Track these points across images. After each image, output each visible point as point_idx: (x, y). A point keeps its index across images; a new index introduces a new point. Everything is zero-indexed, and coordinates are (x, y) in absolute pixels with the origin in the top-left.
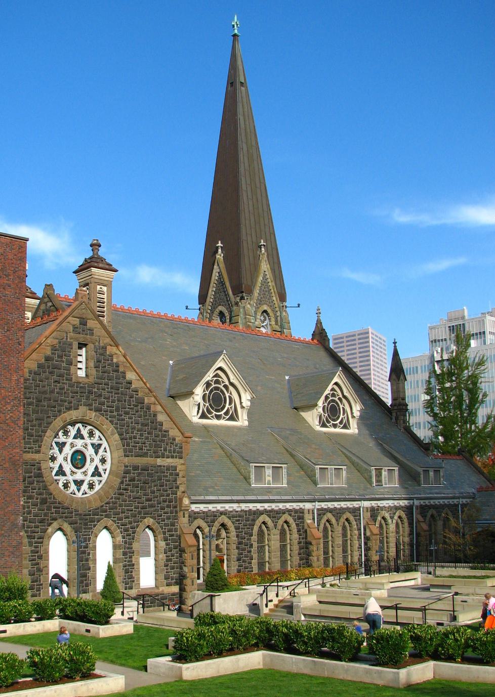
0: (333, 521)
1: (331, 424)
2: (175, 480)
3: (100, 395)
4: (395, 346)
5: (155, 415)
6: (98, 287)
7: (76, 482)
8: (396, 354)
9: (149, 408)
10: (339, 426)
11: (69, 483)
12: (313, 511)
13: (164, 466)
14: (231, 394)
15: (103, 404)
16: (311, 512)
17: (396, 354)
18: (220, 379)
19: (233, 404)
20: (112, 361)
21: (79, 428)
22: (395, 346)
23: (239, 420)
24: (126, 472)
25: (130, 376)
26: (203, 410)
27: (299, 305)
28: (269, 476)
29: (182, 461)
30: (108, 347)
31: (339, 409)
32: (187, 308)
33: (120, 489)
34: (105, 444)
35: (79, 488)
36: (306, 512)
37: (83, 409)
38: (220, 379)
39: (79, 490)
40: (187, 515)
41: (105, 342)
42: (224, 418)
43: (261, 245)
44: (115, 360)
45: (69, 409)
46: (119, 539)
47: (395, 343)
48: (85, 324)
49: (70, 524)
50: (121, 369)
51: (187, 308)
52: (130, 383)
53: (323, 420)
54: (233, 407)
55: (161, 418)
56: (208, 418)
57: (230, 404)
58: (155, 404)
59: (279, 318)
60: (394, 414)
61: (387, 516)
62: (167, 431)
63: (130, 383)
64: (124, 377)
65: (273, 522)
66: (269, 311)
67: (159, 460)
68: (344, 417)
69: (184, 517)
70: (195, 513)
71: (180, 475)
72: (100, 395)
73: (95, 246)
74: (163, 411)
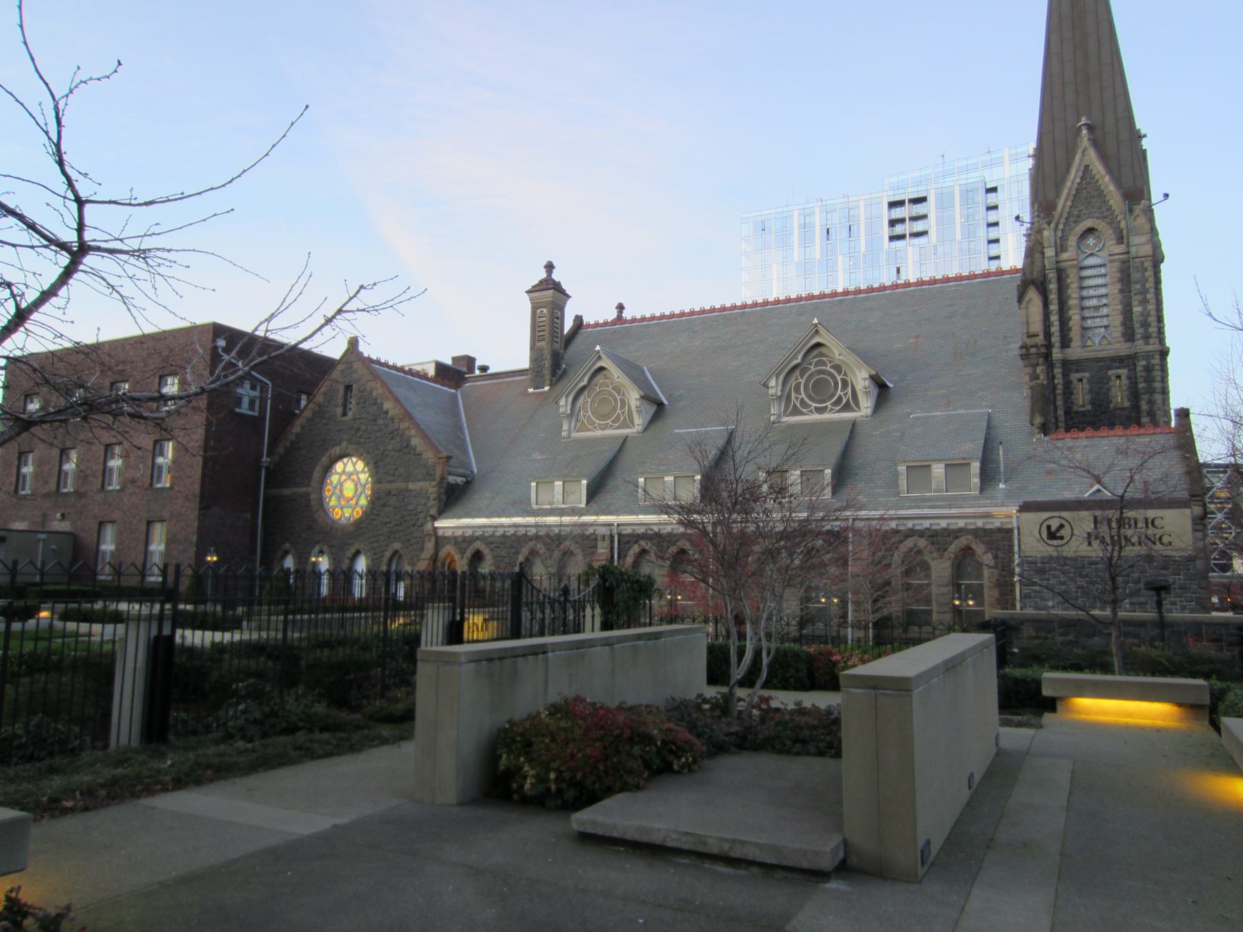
1: (829, 406)
2: (425, 505)
3: (358, 429)
5: (409, 440)
6: (539, 311)
9: (402, 435)
15: (361, 437)
20: (372, 394)
24: (379, 499)
27: (1166, 196)
29: (433, 483)
33: (372, 514)
36: (599, 538)
37: (344, 444)
40: (433, 539)
42: (611, 426)
43: (1080, 127)
44: (374, 394)
45: (333, 446)
46: (369, 561)
48: (351, 368)
49: (329, 547)
50: (379, 401)
52: (387, 412)
53: (795, 405)
55: (415, 441)
57: (623, 406)
58: (409, 428)
59: (1125, 231)
62: (420, 455)
63: (387, 412)
64: (382, 408)
65: (549, 549)
67: (410, 484)
68: (845, 394)
71: (432, 498)
72: (358, 429)
73: (550, 267)
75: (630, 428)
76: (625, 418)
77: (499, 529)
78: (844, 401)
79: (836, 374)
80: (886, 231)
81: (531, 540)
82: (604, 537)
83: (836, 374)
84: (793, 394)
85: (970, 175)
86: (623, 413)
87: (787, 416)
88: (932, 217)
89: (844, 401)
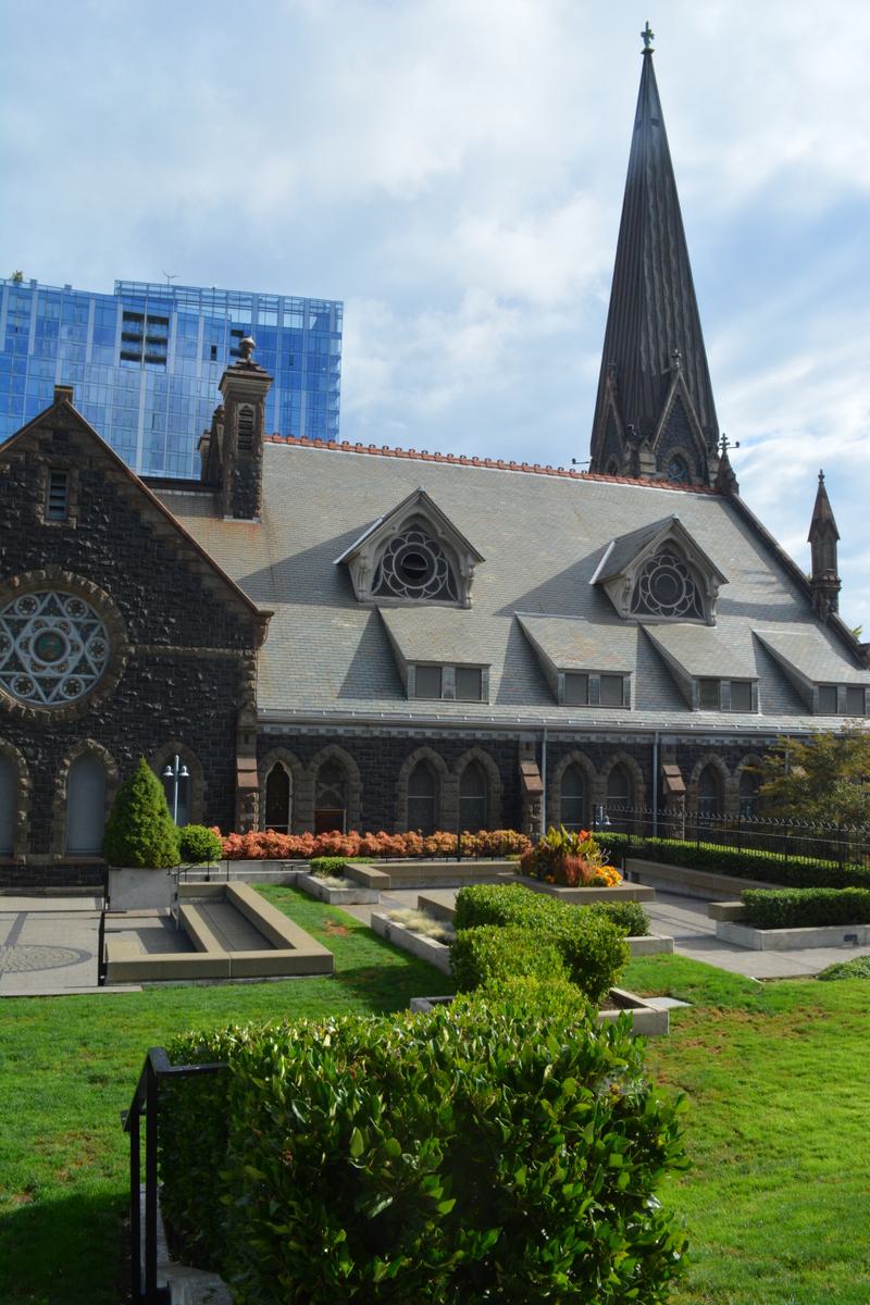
0: (589, 764)
4: (821, 483)
7: (42, 681)
8: (822, 495)
10: (677, 613)
11: (31, 682)
12: (539, 745)
13: (211, 661)
14: (443, 556)
16: (534, 747)
17: (822, 495)
18: (420, 534)
19: (447, 573)
21: (53, 597)
22: (821, 483)
23: (457, 597)
25: (147, 516)
26: (384, 583)
28: (449, 684)
30: (109, 474)
31: (681, 584)
32: (574, 461)
34: (101, 624)
35: (47, 690)
38: (420, 534)
39: (47, 694)
40: (253, 739)
41: (101, 464)
42: (426, 595)
44: (120, 493)
47: (821, 477)
51: (574, 461)
53: (642, 602)
54: (447, 578)
56: (394, 595)
57: (441, 571)
60: (815, 596)
61: (721, 763)
66: (687, 456)
68: (690, 599)
69: (246, 742)
70: (272, 737)
74: (212, 572)
75: (451, 599)
76: (445, 587)
77: (371, 729)
78: (689, 606)
79: (681, 577)
80: (119, 345)
81: (421, 745)
82: (528, 744)
83: (681, 577)
84: (640, 589)
85: (216, 310)
86: (442, 579)
87: (636, 612)
88: (172, 343)
89: (689, 606)
